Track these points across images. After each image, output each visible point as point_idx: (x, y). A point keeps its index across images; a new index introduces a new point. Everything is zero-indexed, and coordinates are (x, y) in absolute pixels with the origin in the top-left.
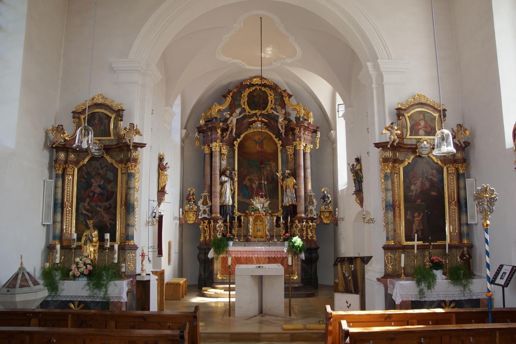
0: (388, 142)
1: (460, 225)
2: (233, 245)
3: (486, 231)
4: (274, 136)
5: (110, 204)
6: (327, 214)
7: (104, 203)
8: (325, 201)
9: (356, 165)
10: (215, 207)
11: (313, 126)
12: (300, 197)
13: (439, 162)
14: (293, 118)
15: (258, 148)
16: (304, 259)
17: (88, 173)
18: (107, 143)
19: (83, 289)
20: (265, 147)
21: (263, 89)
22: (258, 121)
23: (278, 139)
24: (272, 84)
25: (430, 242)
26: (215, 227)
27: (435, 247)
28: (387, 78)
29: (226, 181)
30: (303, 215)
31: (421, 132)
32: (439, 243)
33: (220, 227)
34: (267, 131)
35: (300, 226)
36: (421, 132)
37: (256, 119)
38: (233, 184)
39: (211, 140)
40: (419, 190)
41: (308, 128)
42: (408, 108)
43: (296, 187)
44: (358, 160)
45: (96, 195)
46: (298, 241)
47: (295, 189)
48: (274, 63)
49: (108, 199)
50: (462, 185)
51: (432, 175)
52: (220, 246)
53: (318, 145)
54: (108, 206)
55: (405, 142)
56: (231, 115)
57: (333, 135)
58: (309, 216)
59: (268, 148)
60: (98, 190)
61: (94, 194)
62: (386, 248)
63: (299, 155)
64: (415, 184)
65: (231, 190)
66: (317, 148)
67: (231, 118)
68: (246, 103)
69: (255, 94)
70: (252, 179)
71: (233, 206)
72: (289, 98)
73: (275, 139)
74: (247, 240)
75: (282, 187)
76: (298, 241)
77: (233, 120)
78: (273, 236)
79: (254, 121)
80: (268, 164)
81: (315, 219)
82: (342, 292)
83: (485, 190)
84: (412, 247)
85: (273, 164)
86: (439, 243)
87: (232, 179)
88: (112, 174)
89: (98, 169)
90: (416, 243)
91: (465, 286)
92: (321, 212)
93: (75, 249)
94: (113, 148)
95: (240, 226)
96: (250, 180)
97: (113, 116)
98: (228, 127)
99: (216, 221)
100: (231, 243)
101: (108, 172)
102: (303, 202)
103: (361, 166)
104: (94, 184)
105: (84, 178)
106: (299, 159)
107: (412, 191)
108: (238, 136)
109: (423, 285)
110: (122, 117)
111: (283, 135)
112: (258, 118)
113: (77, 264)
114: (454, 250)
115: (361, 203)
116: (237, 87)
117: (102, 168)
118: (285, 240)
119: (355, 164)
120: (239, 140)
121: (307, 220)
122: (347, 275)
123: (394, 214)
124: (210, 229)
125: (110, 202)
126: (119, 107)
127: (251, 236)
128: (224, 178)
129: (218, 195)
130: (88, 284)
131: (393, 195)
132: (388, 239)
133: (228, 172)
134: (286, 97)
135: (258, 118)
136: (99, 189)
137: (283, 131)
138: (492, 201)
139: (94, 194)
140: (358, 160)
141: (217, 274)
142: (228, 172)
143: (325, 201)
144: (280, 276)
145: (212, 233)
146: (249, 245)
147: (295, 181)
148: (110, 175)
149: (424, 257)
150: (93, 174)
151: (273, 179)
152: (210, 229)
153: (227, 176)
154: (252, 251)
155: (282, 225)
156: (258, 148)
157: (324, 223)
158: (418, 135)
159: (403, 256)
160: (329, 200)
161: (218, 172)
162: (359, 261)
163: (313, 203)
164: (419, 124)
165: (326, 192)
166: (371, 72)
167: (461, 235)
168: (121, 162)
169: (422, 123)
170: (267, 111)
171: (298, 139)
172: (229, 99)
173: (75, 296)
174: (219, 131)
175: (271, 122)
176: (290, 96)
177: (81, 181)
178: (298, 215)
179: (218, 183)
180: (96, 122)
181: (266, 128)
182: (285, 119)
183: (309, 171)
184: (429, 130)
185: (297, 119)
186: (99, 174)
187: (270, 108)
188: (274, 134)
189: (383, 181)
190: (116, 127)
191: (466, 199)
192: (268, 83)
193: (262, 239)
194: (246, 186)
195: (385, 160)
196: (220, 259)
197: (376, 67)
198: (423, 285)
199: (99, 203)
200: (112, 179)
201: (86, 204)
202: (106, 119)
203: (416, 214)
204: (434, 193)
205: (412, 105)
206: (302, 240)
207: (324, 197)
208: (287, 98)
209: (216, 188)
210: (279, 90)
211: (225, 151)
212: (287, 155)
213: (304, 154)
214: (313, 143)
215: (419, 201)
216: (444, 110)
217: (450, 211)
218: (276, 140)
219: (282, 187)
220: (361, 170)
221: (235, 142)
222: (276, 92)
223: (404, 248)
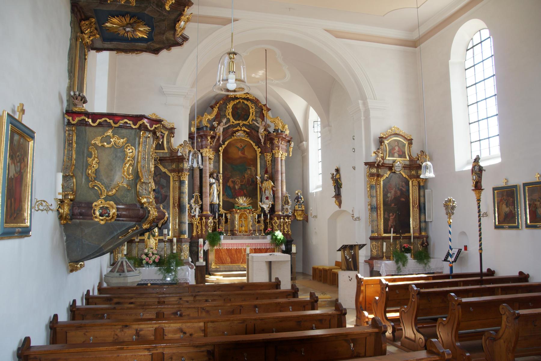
0: (375, 162)
1: (420, 222)
2: (224, 238)
3: (450, 226)
4: (254, 144)
6: (300, 213)
8: (298, 201)
9: (336, 174)
10: (206, 205)
11: (288, 137)
12: (278, 197)
13: (407, 177)
14: (271, 130)
15: (240, 154)
16: (284, 249)
18: (161, 155)
19: (156, 273)
20: (246, 153)
21: (246, 102)
22: (241, 130)
25: (400, 234)
26: (206, 223)
27: (405, 238)
28: (372, 113)
29: (214, 183)
30: (280, 213)
31: (396, 155)
32: (406, 235)
33: (211, 223)
34: (248, 140)
35: (278, 223)
36: (396, 155)
37: (240, 129)
38: (219, 185)
39: (202, 145)
40: (393, 197)
41: (285, 138)
42: (388, 137)
43: (274, 189)
44: (337, 170)
46: (279, 235)
47: (273, 191)
48: (260, 82)
50: (422, 194)
51: (402, 186)
52: (214, 239)
53: (291, 153)
55: (386, 162)
56: (219, 124)
57: (305, 145)
58: (285, 214)
59: (248, 154)
62: (372, 238)
63: (278, 162)
64: (391, 193)
65: (218, 191)
66: (291, 156)
67: (219, 127)
68: (230, 114)
69: (239, 106)
70: (234, 181)
71: (219, 205)
74: (233, 233)
75: (261, 189)
76: (279, 235)
77: (220, 129)
79: (238, 131)
81: (290, 216)
82: (345, 270)
83: (450, 201)
84: (389, 238)
85: (253, 169)
86: (406, 235)
87: (219, 181)
88: (165, 181)
90: (392, 235)
91: (426, 264)
92: (295, 210)
93: (138, 242)
94: (166, 160)
95: (226, 221)
96: (233, 182)
97: (166, 133)
98: (216, 135)
99: (207, 218)
100: (222, 237)
102: (280, 202)
103: (340, 175)
106: (278, 165)
107: (388, 197)
108: (224, 142)
109: (400, 264)
110: (173, 133)
112: (241, 128)
113: (147, 255)
114: (416, 240)
115: (340, 204)
116: (222, 99)
118: (267, 234)
119: (335, 173)
120: (223, 146)
121: (284, 217)
122: (348, 258)
123: (377, 214)
124: (201, 225)
126: (171, 126)
127: (237, 231)
128: (213, 181)
129: (208, 195)
130: (160, 270)
131: (377, 200)
132: (372, 232)
133: (215, 175)
135: (241, 128)
137: (262, 141)
138: (453, 208)
140: (337, 170)
141: (211, 265)
142: (215, 175)
143: (298, 201)
144: (287, 261)
145: (204, 228)
146: (236, 239)
147: (272, 184)
148: (163, 181)
149: (396, 245)
151: (253, 181)
152: (201, 225)
153: (214, 178)
154: (241, 244)
155: (262, 222)
157: (297, 220)
158: (393, 157)
159: (385, 244)
160: (302, 200)
161: (208, 175)
162: (357, 248)
163: (288, 202)
164: (395, 149)
165: (299, 194)
166: (361, 108)
167: (420, 229)
168: (171, 171)
169: (397, 148)
171: (277, 148)
172: (216, 110)
173: (149, 280)
174: (209, 138)
175: (252, 132)
176: (268, 110)
178: (276, 213)
179: (208, 185)
181: (247, 137)
182: (265, 130)
183: (284, 175)
184: (401, 153)
185: (276, 130)
188: (254, 142)
189: (368, 189)
190: (169, 142)
191: (425, 204)
192: (250, 98)
194: (229, 187)
195: (372, 175)
196: (214, 251)
197: (365, 104)
198: (400, 264)
200: (165, 184)
203: (391, 214)
204: (403, 199)
205: (391, 135)
206: (283, 234)
207: (298, 198)
209: (206, 189)
210: (260, 104)
211: (212, 156)
212: (265, 162)
213: (281, 160)
214: (287, 151)
215: (393, 204)
216: (412, 139)
217: (413, 212)
218: (256, 148)
219: (261, 189)
220: (340, 178)
221: (220, 149)
223: (384, 239)
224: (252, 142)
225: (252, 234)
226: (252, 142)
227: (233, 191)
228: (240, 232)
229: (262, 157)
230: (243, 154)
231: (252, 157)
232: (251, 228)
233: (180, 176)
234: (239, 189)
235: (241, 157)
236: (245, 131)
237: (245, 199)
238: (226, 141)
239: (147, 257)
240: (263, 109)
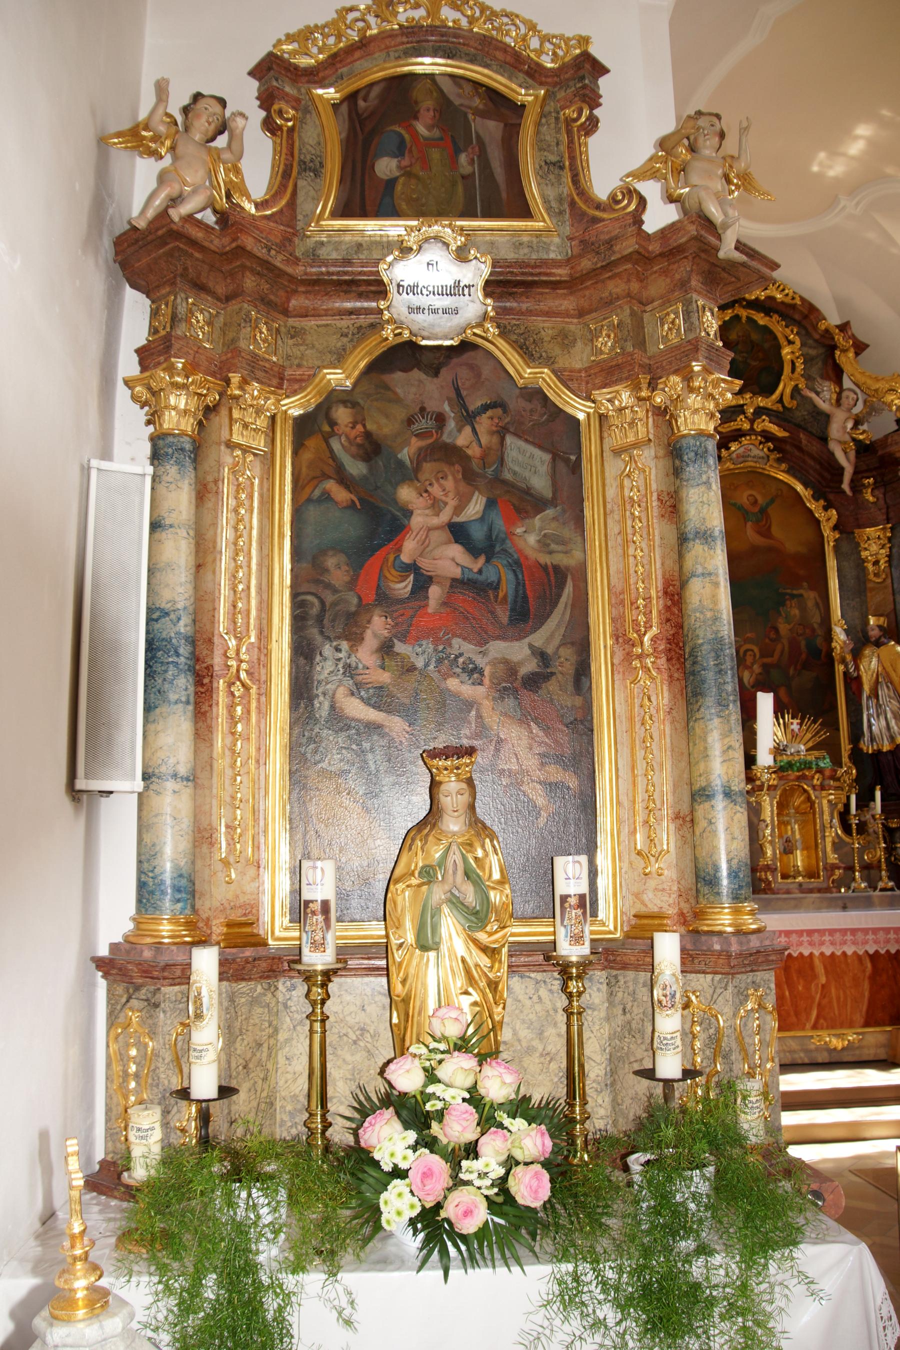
5: (542, 656)
7: (498, 648)
17: (371, 448)
20: (776, 531)
21: (761, 319)
23: (822, 502)
24: (798, 302)
37: (746, 426)
45: (435, 592)
49: (524, 616)
54: (530, 666)
59: (788, 538)
60: (451, 560)
61: (423, 582)
72: (857, 354)
73: (812, 505)
78: (851, 869)
80: (793, 596)
85: (811, 597)
88: (541, 459)
89: (440, 419)
101: (509, 439)
104: (418, 521)
105: (344, 480)
111: (846, 486)
117: (469, 418)
125: (538, 638)
134: (844, 351)
136: (456, 551)
139: (423, 582)
148: (528, 463)
150: (405, 454)
170: (781, 400)
177: (326, 497)
180: (421, 129)
186: (450, 454)
187: (788, 391)
188: (806, 485)
193: (814, 883)
199: (462, 647)
200: (540, 483)
201: (366, 655)
202: (483, 114)
208: (851, 354)
210: (822, 326)
222: (808, 334)
224: (799, 488)
225: (838, 884)
226: (799, 488)
228: (785, 876)
229: (845, 547)
230: (766, 532)
232: (833, 858)
233: (661, 412)
236: (767, 436)
237: (795, 726)
239: (428, 1143)
240: (834, 347)
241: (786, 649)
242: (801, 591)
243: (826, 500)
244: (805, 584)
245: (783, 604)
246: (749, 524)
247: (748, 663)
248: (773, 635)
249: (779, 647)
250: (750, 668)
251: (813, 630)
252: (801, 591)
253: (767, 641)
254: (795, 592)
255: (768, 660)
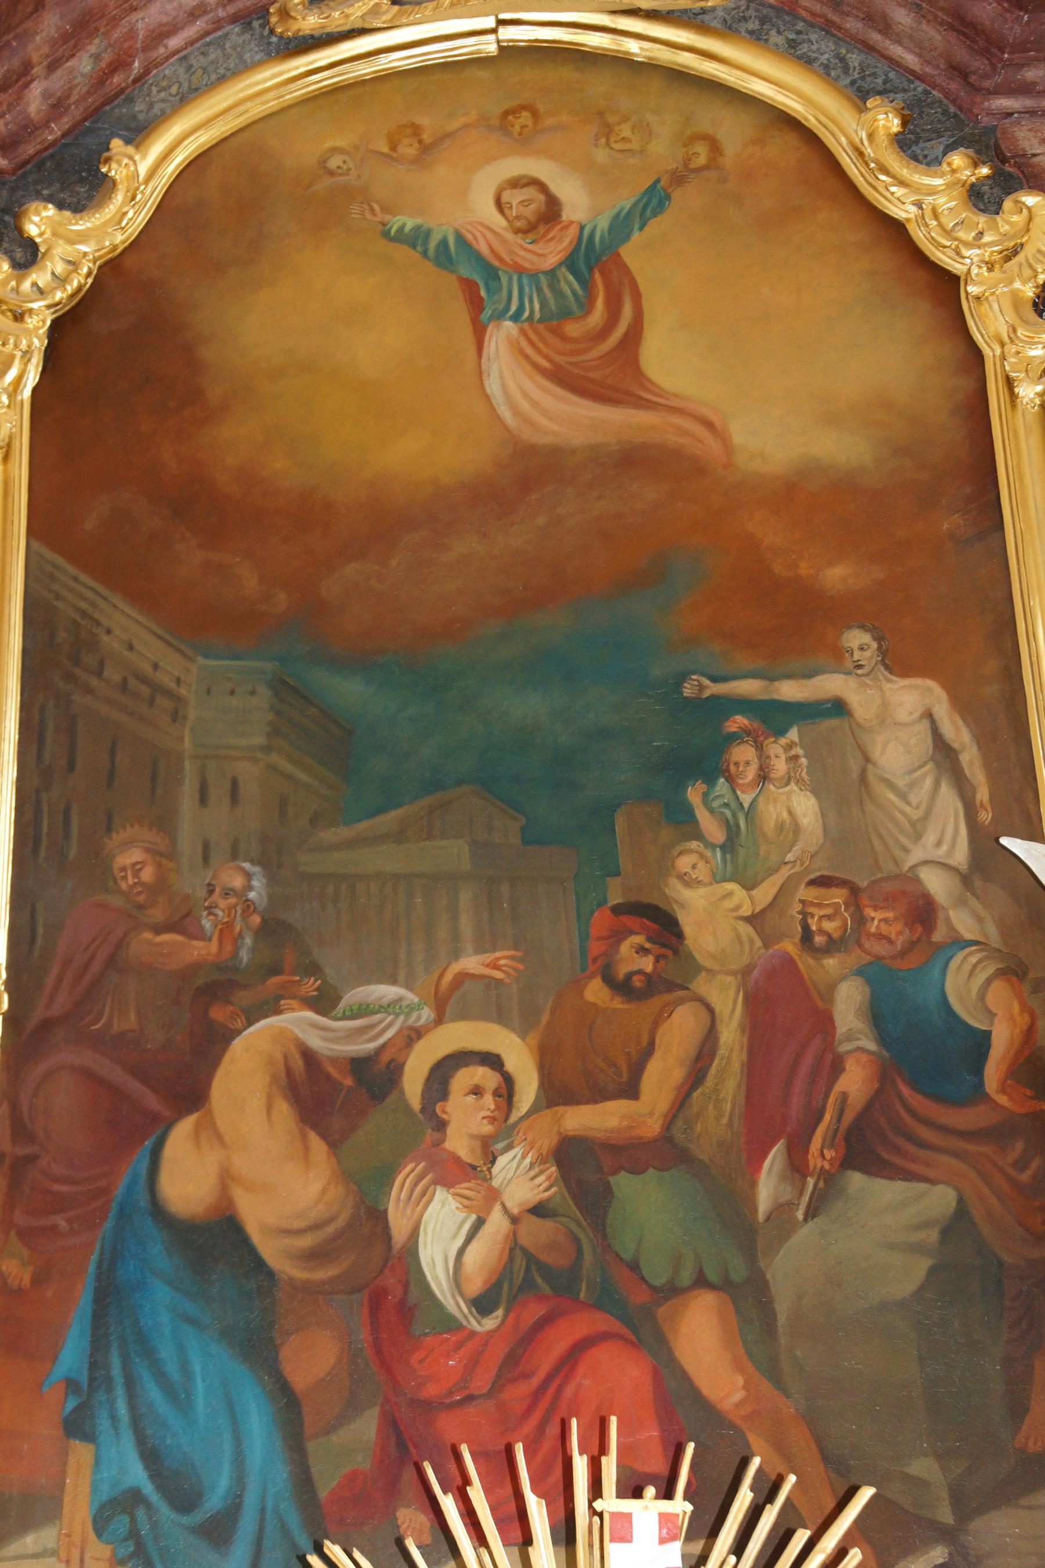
4: (863, 132)
15: (513, 388)
20: (669, 359)
70: (375, 1077)
80: (775, 717)
96: (333, 1098)
156: (513, 388)
194: (216, 1243)
218: (927, 197)
227: (313, 1358)
230: (611, 373)
231: (843, 449)
234: (526, 1281)
235: (531, 472)
238: (137, 133)
241: (731, 1035)
242: (831, 684)
243: (988, 146)
244: (858, 640)
245: (708, 763)
246: (502, 335)
247: (459, 1143)
248: (634, 957)
249: (680, 1030)
250: (467, 1174)
251: (923, 912)
252: (831, 684)
253: (596, 991)
254: (790, 691)
255: (597, 1119)
